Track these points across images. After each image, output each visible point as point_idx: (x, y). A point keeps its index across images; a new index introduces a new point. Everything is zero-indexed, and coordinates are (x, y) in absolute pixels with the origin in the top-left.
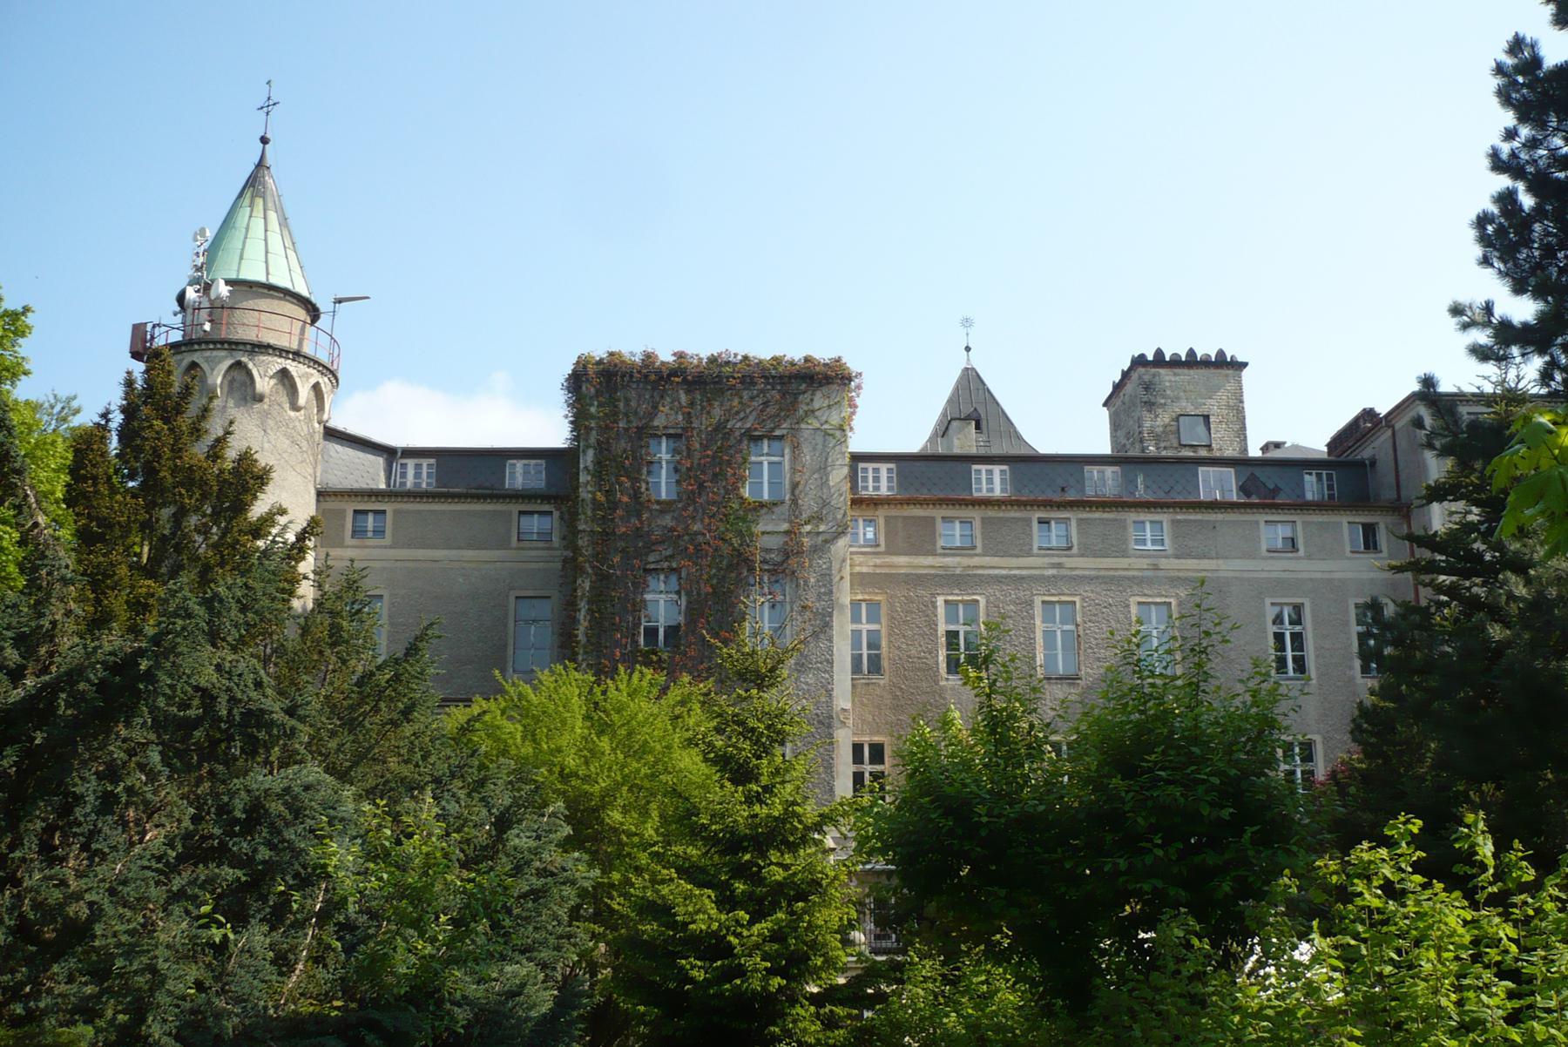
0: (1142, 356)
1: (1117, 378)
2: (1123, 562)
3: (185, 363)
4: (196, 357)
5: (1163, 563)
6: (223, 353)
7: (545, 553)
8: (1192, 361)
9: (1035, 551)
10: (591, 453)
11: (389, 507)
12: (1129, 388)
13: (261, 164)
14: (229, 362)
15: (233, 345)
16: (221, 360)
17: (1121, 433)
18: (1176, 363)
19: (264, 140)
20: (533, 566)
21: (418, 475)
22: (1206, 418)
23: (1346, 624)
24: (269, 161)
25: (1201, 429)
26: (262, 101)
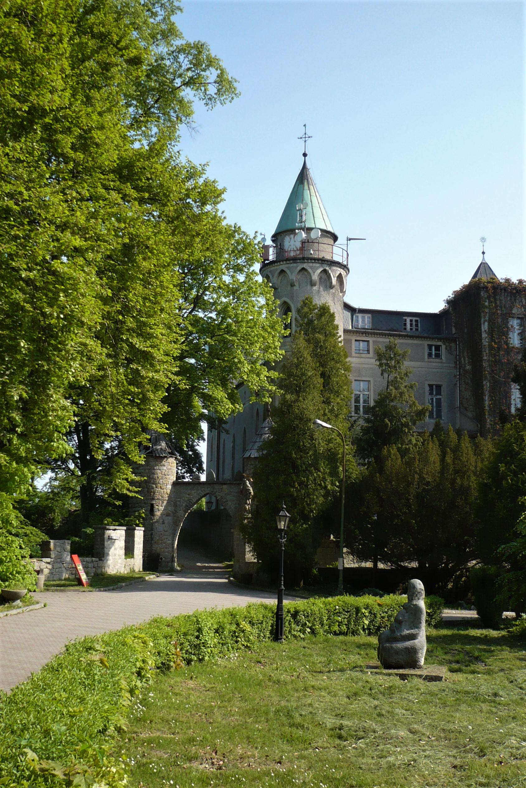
3: (299, 268)
4: (305, 266)
6: (318, 265)
7: (439, 364)
10: (486, 324)
11: (371, 339)
14: (321, 269)
15: (323, 261)
16: (317, 268)
19: (305, 155)
20: (434, 370)
24: (308, 165)
26: (301, 134)
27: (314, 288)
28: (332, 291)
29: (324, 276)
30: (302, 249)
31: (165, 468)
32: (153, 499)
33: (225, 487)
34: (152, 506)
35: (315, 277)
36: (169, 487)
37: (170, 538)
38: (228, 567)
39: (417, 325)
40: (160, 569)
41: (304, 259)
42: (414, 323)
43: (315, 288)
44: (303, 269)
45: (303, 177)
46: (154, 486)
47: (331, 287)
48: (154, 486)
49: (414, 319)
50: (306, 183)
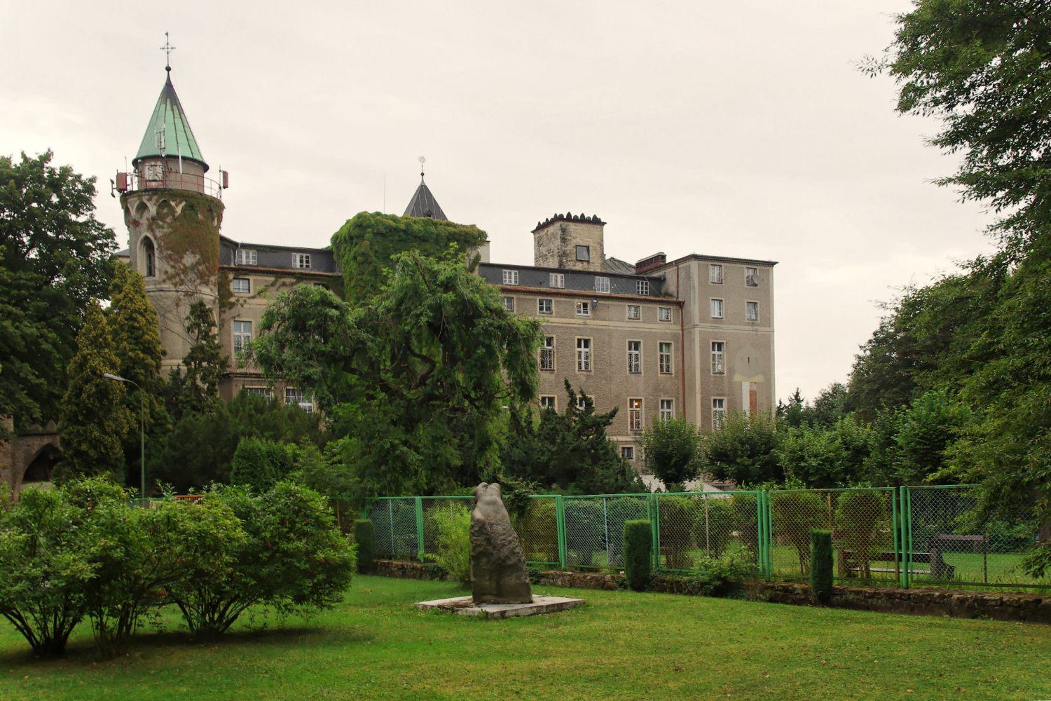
0: (562, 216)
1: (543, 221)
2: (573, 321)
5: (588, 322)
8: (583, 220)
9: (538, 314)
12: (551, 229)
17: (544, 250)
18: (576, 220)
19: (168, 69)
21: (248, 257)
22: (588, 247)
23: (656, 351)
25: (585, 253)
26: (163, 44)
39: (307, 262)
42: (304, 259)
49: (304, 255)
50: (168, 103)
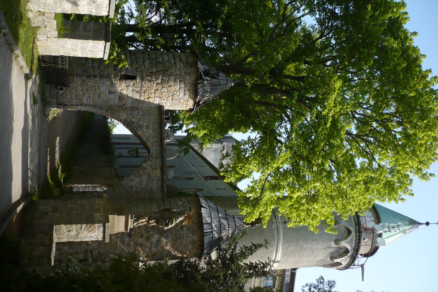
4: (353, 234)
6: (353, 246)
13: (419, 224)
14: (349, 248)
16: (351, 246)
24: (420, 227)
27: (333, 243)
28: (328, 259)
29: (342, 251)
30: (366, 229)
31: (181, 95)
32: (142, 79)
33: (158, 172)
34: (133, 78)
35: (344, 244)
36: (157, 101)
37: (90, 101)
38: (54, 172)
40: (48, 87)
41: (359, 232)
43: (333, 244)
44: (350, 232)
45: (413, 223)
46: (159, 81)
47: (332, 258)
48: (159, 81)
